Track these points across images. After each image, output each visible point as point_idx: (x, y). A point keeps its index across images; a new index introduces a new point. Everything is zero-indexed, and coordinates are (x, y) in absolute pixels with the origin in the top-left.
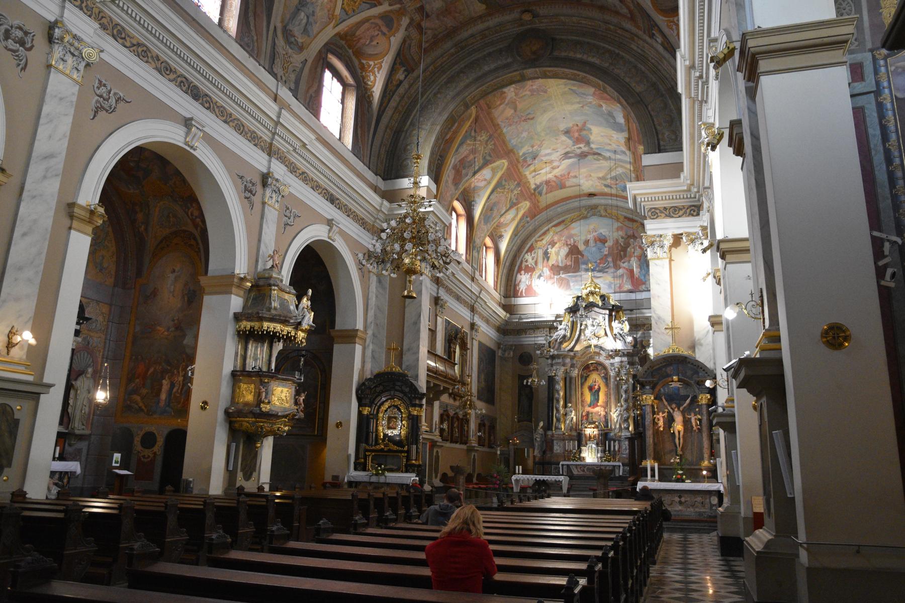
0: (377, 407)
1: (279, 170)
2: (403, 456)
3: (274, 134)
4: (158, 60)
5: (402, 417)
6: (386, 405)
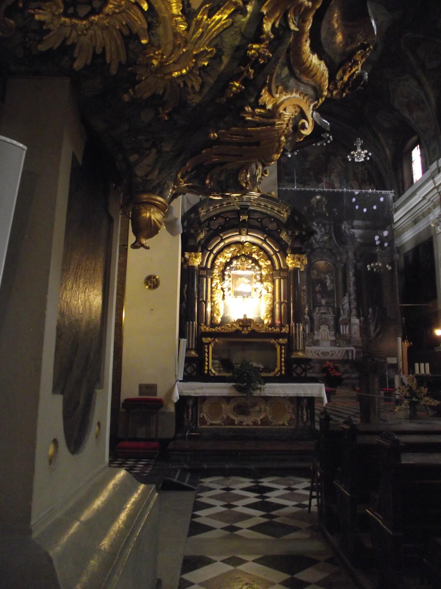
0: (212, 256)
2: (281, 345)
5: (261, 274)
6: (228, 254)
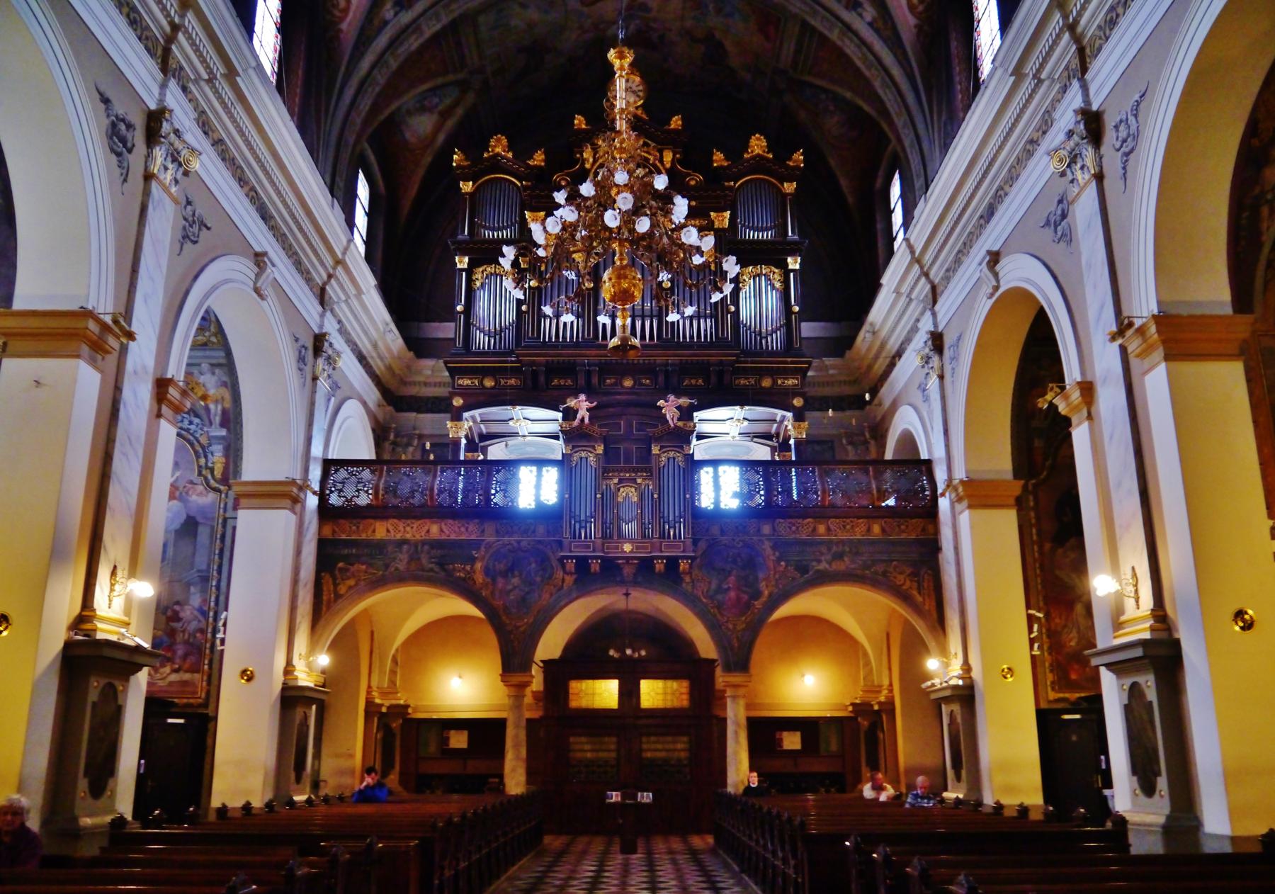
1: (330, 326)
3: (330, 276)
4: (234, 164)
